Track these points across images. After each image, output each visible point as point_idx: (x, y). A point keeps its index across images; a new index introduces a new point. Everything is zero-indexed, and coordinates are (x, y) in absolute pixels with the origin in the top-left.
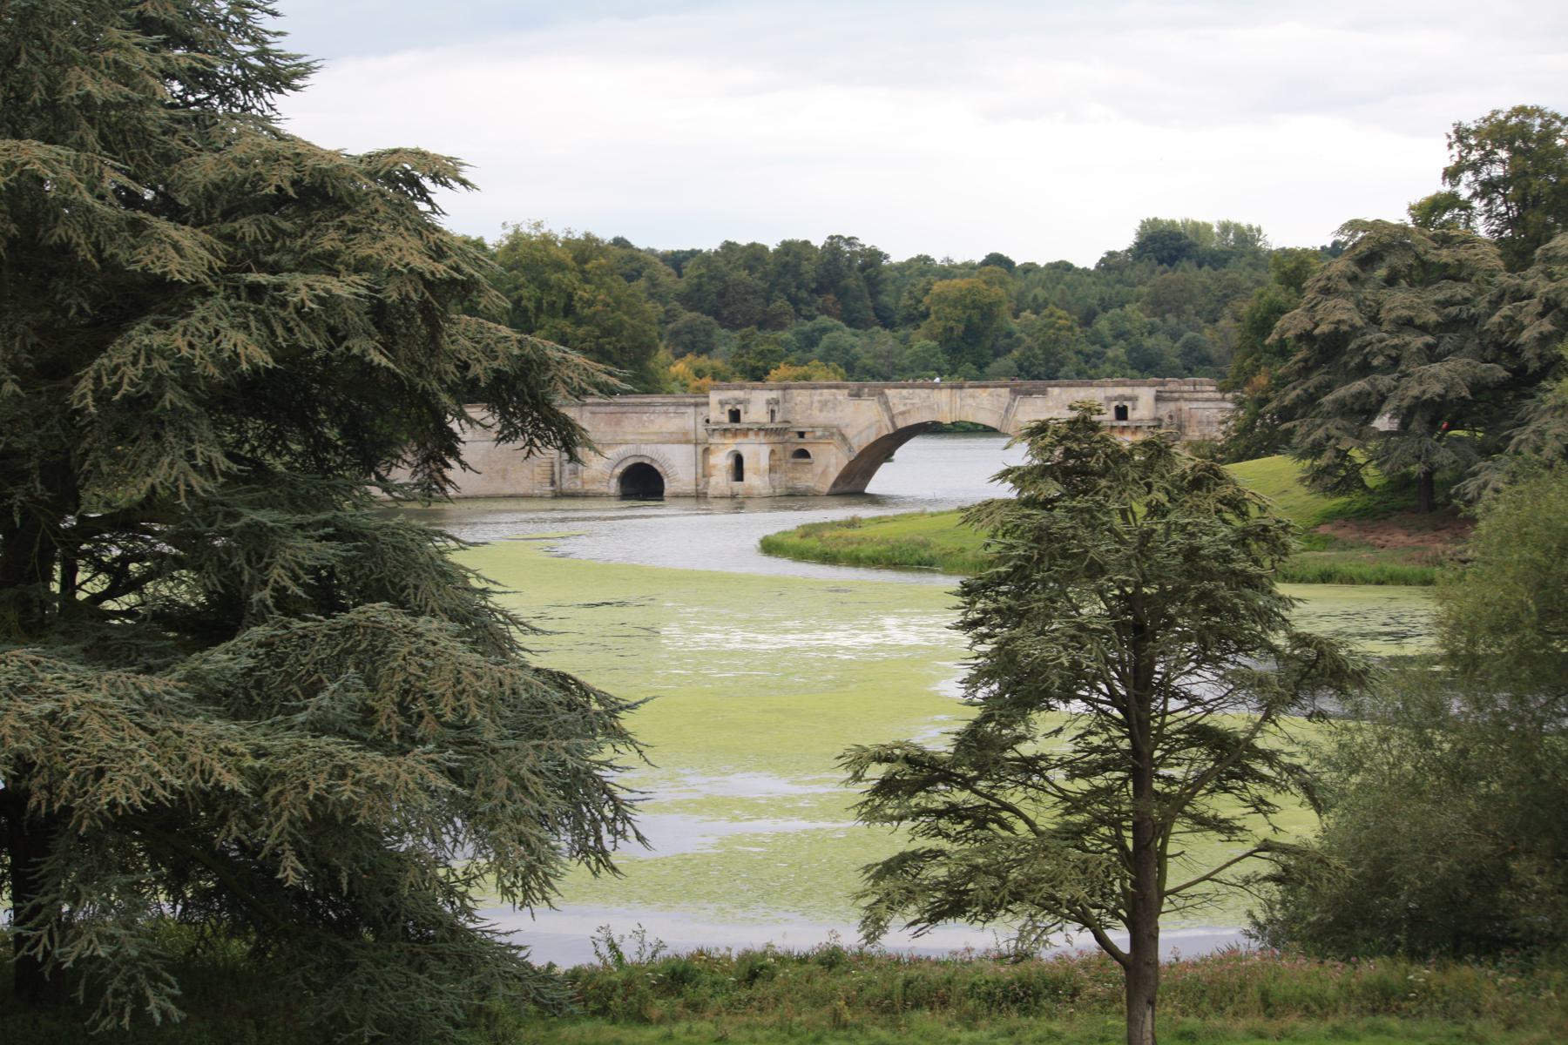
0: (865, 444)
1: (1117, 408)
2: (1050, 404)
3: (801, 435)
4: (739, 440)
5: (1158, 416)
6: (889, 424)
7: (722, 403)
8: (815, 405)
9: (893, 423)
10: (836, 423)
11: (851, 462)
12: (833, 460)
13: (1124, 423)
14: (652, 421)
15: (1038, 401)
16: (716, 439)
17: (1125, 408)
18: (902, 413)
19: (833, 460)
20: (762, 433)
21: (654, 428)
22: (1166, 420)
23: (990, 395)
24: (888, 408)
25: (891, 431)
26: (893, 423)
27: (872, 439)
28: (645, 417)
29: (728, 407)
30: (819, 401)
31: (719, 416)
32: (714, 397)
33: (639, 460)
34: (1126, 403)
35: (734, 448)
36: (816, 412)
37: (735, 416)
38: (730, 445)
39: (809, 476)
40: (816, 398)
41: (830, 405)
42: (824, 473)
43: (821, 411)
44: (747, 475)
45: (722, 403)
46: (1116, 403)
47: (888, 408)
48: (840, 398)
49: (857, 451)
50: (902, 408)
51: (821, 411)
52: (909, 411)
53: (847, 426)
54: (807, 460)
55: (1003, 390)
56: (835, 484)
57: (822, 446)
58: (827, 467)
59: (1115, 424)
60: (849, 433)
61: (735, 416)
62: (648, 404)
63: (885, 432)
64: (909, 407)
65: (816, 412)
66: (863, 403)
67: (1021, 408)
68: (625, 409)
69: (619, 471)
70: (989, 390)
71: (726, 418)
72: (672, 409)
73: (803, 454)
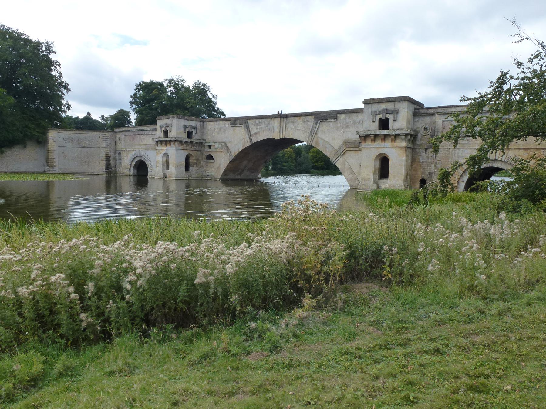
0: (237, 152)
1: (380, 120)
2: (339, 125)
3: (210, 146)
4: (168, 147)
5: (415, 128)
6: (249, 140)
7: (161, 127)
8: (216, 130)
9: (251, 140)
10: (224, 140)
11: (232, 162)
12: (223, 161)
13: (385, 132)
14: (144, 139)
15: (331, 124)
16: (160, 147)
17: (387, 120)
18: (256, 134)
19: (223, 161)
20: (176, 143)
21: (144, 142)
22: (422, 132)
23: (303, 121)
24: (249, 131)
25: (250, 144)
26: (251, 140)
27: (240, 150)
28: (142, 137)
29: (163, 129)
30: (218, 128)
31: (159, 134)
32: (159, 123)
33: (140, 158)
34: (388, 116)
35: (165, 151)
36: (216, 134)
37: (166, 133)
38: (164, 149)
39: (213, 169)
40: (217, 126)
41: (222, 130)
42: (219, 167)
43: (218, 133)
44: (171, 166)
45: (161, 127)
46: (380, 116)
47: (249, 131)
48: (227, 126)
49: (233, 156)
50: (256, 131)
51: (218, 133)
52: (259, 133)
53: (230, 142)
54: (211, 161)
55: (310, 117)
56: (225, 173)
57: (218, 153)
58: (220, 164)
59: (378, 132)
60: (229, 145)
61: (166, 133)
62: (142, 130)
63: (247, 145)
64: (259, 130)
65: (216, 134)
66: (237, 128)
67: (320, 129)
68: (135, 133)
69: (134, 163)
70: (302, 118)
71: (162, 135)
72: (150, 132)
73: (210, 157)
